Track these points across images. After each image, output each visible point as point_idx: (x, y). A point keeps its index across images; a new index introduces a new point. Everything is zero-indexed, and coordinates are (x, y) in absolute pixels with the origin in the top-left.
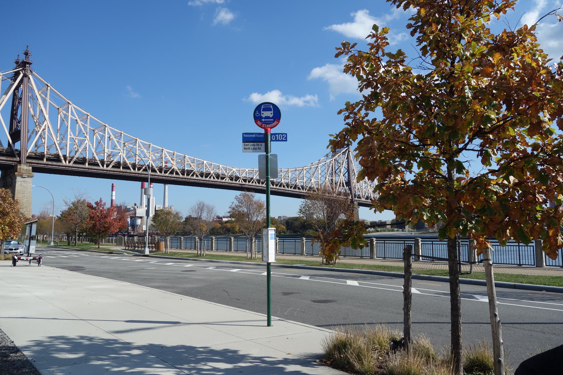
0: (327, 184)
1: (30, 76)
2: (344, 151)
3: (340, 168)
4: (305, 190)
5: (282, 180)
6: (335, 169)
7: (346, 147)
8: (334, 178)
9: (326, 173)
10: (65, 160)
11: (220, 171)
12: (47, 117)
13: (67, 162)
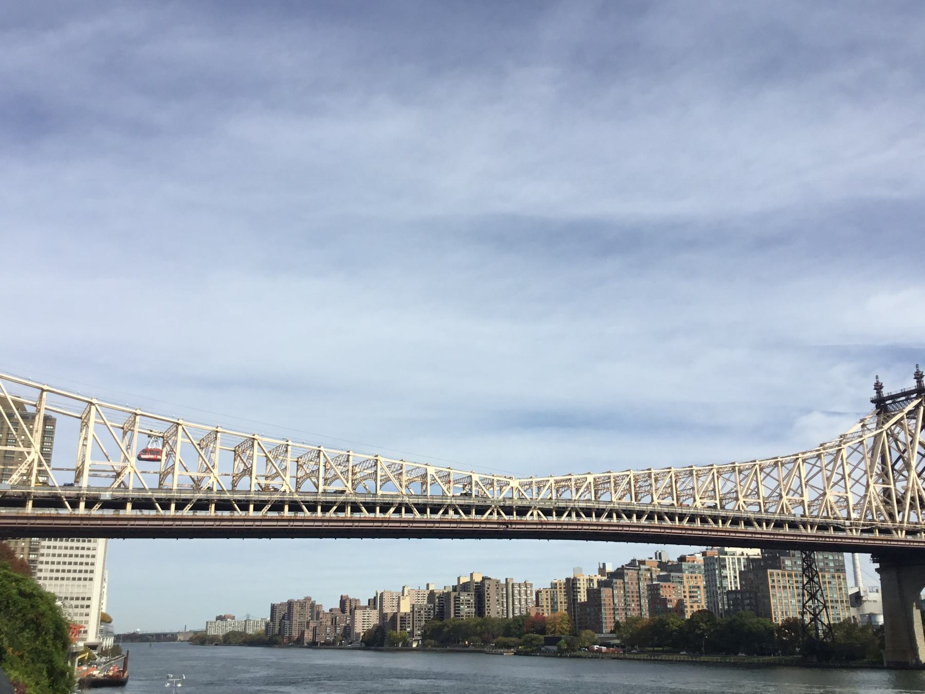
0: (874, 504)
2: (911, 406)
3: (906, 455)
4: (767, 525)
5: (695, 501)
6: (891, 462)
7: (916, 398)
8: (892, 486)
9: (866, 472)
11: (474, 488)
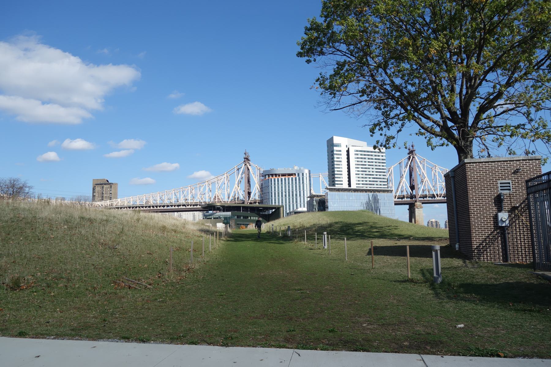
1: (416, 157)
10: (438, 196)
12: (426, 175)
13: (439, 197)
